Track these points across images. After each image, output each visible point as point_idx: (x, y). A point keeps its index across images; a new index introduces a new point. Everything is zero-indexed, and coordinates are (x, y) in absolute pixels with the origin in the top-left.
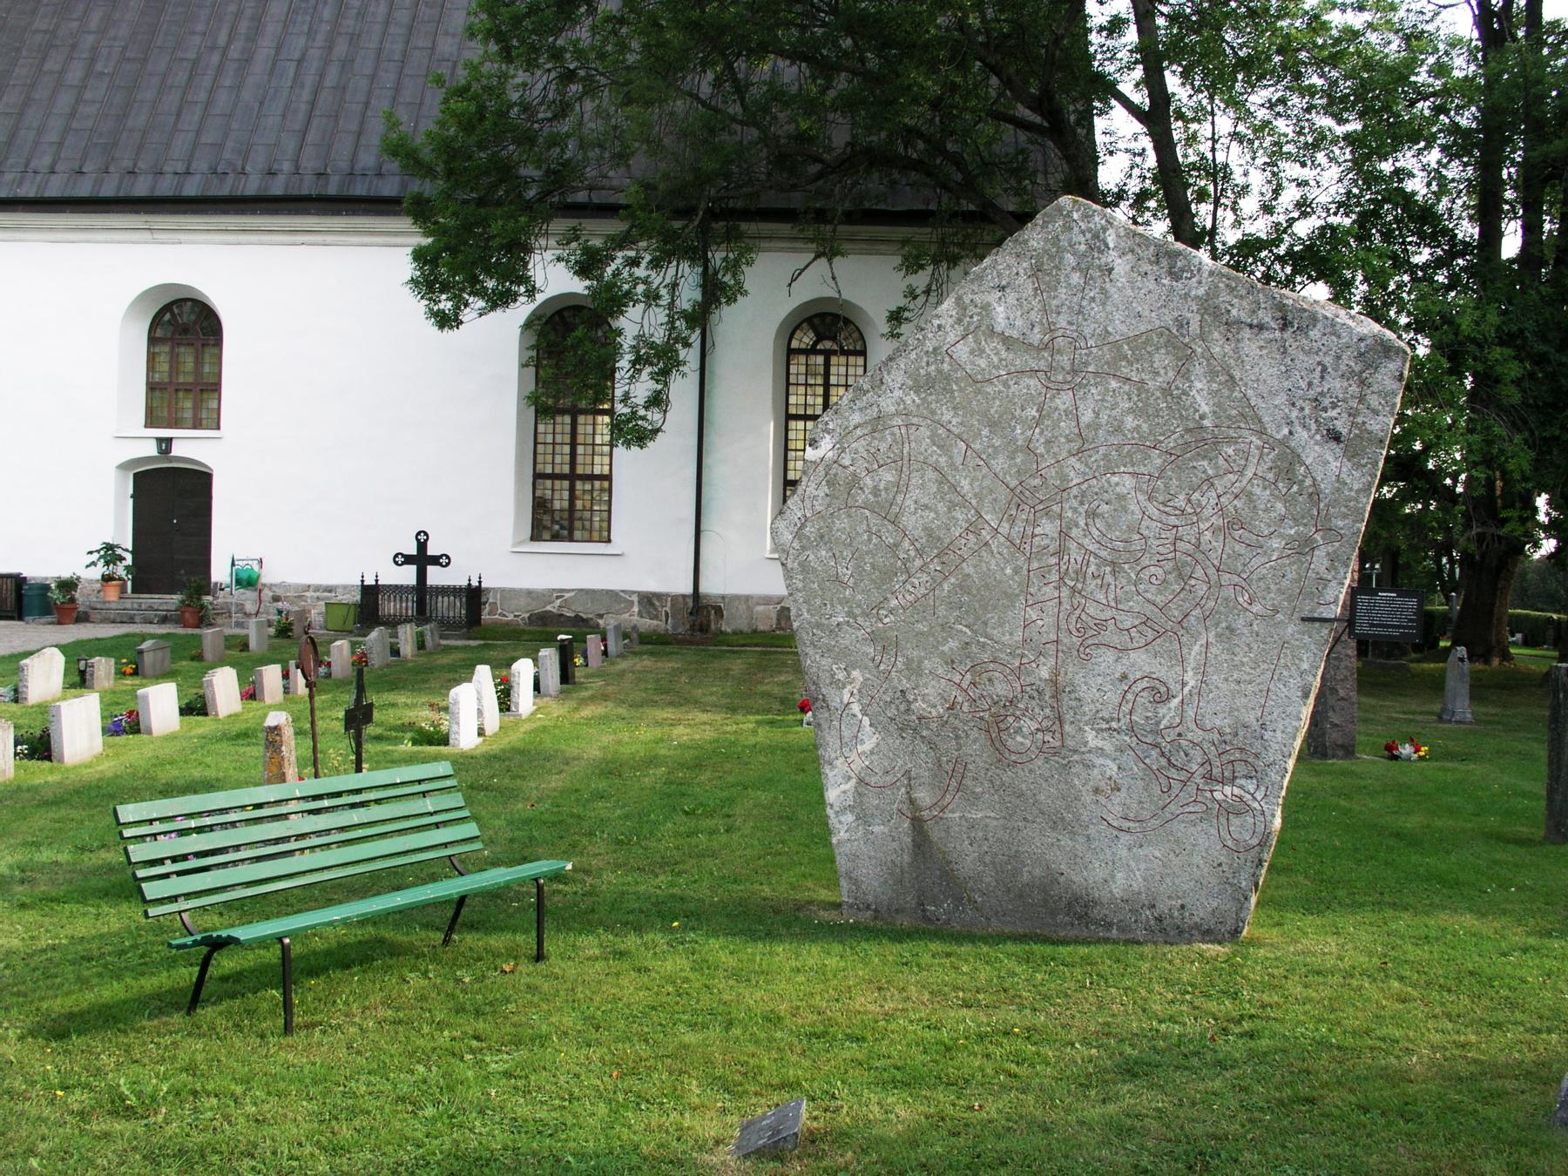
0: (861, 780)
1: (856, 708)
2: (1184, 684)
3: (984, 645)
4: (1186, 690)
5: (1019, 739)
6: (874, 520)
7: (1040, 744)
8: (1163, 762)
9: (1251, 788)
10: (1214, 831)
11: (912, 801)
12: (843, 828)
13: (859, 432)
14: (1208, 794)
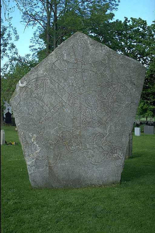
0: (37, 159)
1: (35, 143)
2: (107, 134)
3: (64, 127)
4: (107, 135)
5: (73, 147)
6: (37, 101)
7: (77, 148)
8: (103, 150)
9: (120, 154)
10: (113, 163)
11: (49, 163)
12: (31, 171)
13: (33, 80)
14: (112, 156)
